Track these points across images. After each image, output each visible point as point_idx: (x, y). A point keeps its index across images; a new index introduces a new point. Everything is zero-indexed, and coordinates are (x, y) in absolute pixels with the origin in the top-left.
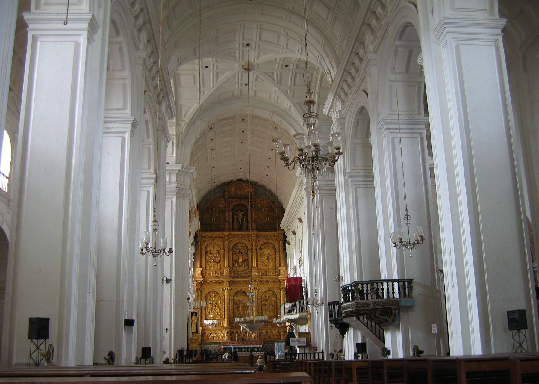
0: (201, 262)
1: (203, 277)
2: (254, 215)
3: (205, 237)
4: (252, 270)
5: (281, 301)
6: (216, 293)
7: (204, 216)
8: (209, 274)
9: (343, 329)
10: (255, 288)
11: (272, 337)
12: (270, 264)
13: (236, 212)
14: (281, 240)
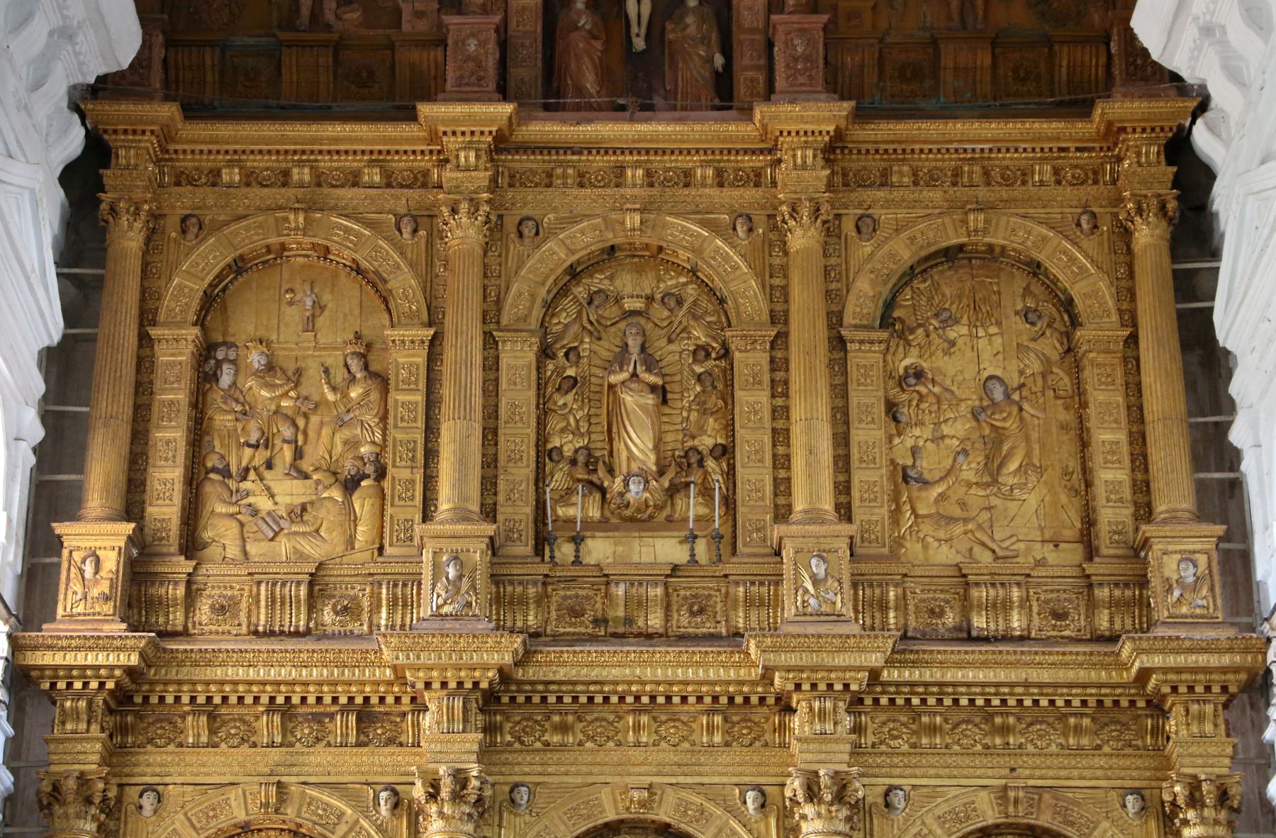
4: (787, 554)
8: (220, 610)
10: (824, 780)
12: (1013, 506)
14: (1140, 211)
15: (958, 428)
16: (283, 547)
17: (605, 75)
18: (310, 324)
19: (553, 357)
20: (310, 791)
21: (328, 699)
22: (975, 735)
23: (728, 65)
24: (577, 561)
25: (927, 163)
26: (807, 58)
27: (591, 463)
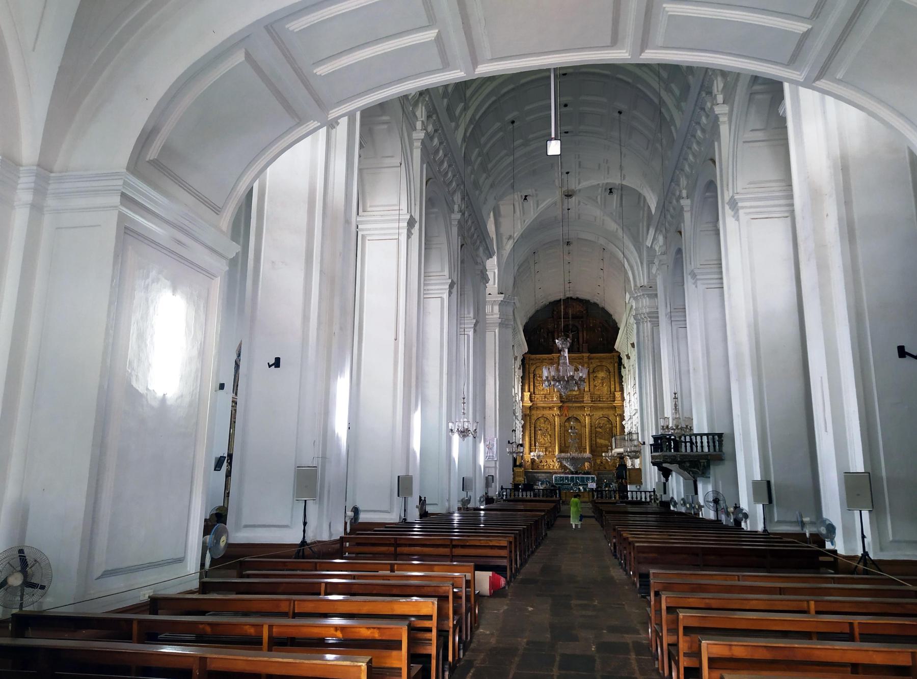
1: (531, 401)
2: (585, 335)
3: (533, 360)
6: (546, 419)
8: (538, 399)
9: (666, 473)
11: (607, 468)
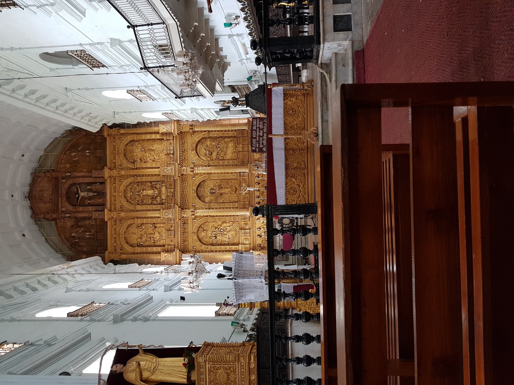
0: (153, 253)
4: (164, 174)
5: (212, 131)
6: (201, 229)
7: (85, 249)
13: (79, 201)
14: (119, 132)
15: (147, 154)
16: (163, 235)
17: (100, 198)
18: (135, 234)
19: (139, 203)
20: (193, 229)
21: (182, 228)
22: (186, 153)
23: (99, 183)
24: (165, 200)
25: (112, 158)
26: (98, 173)
27: (153, 198)
